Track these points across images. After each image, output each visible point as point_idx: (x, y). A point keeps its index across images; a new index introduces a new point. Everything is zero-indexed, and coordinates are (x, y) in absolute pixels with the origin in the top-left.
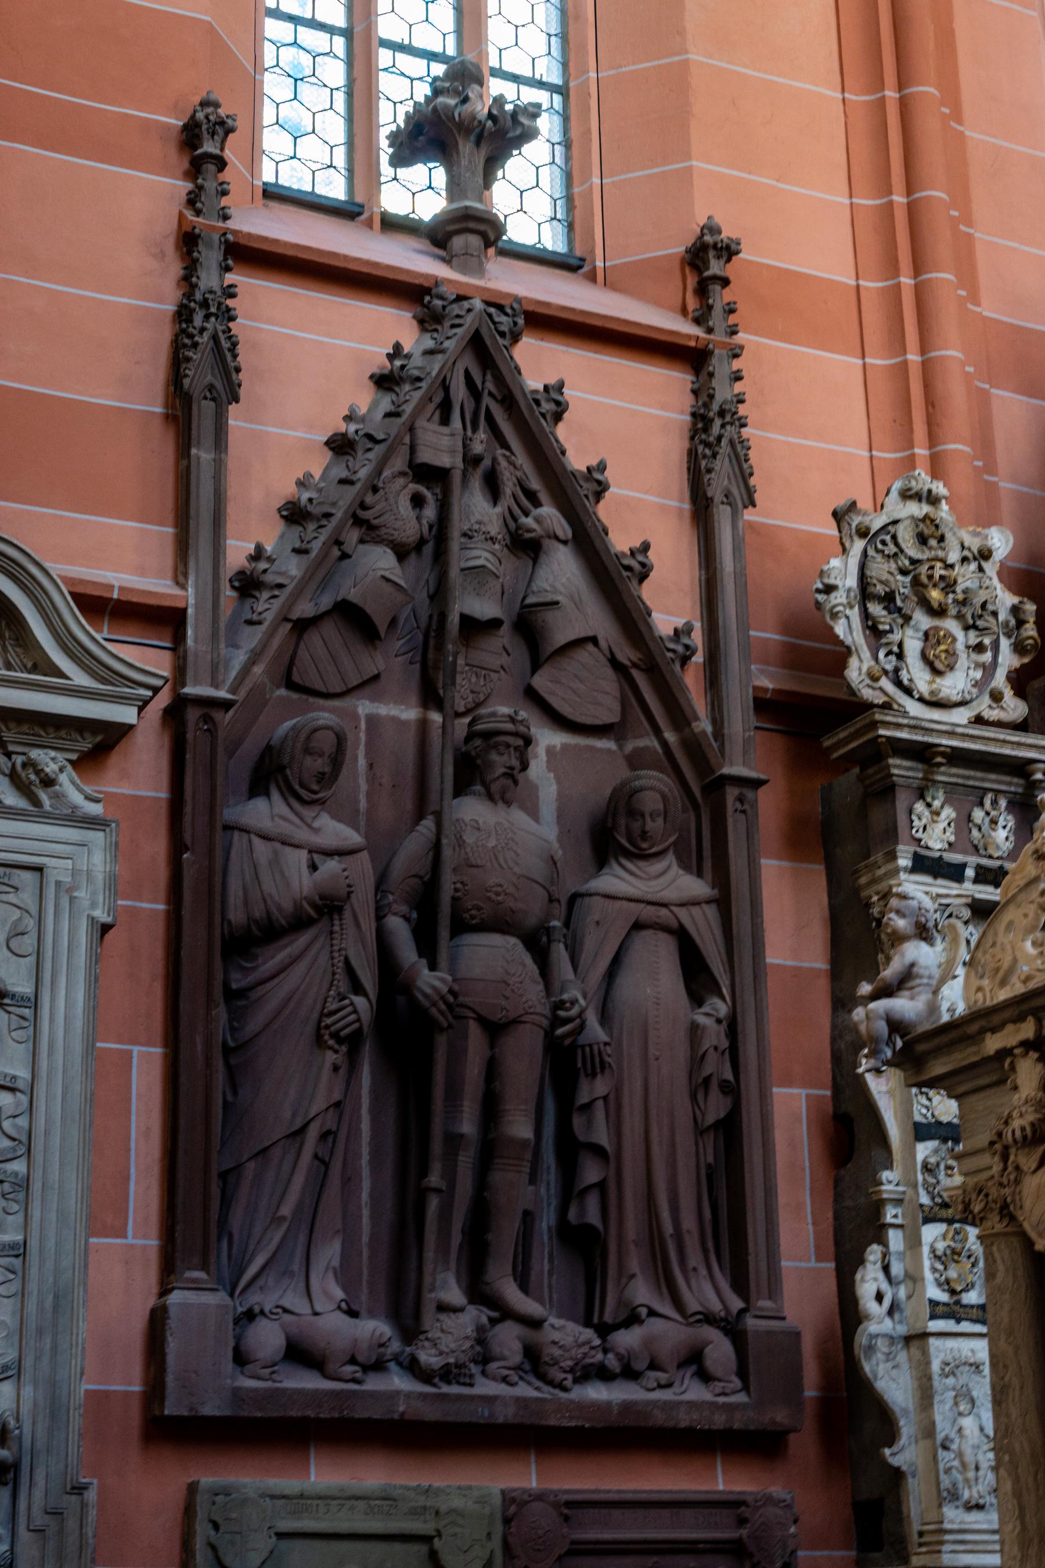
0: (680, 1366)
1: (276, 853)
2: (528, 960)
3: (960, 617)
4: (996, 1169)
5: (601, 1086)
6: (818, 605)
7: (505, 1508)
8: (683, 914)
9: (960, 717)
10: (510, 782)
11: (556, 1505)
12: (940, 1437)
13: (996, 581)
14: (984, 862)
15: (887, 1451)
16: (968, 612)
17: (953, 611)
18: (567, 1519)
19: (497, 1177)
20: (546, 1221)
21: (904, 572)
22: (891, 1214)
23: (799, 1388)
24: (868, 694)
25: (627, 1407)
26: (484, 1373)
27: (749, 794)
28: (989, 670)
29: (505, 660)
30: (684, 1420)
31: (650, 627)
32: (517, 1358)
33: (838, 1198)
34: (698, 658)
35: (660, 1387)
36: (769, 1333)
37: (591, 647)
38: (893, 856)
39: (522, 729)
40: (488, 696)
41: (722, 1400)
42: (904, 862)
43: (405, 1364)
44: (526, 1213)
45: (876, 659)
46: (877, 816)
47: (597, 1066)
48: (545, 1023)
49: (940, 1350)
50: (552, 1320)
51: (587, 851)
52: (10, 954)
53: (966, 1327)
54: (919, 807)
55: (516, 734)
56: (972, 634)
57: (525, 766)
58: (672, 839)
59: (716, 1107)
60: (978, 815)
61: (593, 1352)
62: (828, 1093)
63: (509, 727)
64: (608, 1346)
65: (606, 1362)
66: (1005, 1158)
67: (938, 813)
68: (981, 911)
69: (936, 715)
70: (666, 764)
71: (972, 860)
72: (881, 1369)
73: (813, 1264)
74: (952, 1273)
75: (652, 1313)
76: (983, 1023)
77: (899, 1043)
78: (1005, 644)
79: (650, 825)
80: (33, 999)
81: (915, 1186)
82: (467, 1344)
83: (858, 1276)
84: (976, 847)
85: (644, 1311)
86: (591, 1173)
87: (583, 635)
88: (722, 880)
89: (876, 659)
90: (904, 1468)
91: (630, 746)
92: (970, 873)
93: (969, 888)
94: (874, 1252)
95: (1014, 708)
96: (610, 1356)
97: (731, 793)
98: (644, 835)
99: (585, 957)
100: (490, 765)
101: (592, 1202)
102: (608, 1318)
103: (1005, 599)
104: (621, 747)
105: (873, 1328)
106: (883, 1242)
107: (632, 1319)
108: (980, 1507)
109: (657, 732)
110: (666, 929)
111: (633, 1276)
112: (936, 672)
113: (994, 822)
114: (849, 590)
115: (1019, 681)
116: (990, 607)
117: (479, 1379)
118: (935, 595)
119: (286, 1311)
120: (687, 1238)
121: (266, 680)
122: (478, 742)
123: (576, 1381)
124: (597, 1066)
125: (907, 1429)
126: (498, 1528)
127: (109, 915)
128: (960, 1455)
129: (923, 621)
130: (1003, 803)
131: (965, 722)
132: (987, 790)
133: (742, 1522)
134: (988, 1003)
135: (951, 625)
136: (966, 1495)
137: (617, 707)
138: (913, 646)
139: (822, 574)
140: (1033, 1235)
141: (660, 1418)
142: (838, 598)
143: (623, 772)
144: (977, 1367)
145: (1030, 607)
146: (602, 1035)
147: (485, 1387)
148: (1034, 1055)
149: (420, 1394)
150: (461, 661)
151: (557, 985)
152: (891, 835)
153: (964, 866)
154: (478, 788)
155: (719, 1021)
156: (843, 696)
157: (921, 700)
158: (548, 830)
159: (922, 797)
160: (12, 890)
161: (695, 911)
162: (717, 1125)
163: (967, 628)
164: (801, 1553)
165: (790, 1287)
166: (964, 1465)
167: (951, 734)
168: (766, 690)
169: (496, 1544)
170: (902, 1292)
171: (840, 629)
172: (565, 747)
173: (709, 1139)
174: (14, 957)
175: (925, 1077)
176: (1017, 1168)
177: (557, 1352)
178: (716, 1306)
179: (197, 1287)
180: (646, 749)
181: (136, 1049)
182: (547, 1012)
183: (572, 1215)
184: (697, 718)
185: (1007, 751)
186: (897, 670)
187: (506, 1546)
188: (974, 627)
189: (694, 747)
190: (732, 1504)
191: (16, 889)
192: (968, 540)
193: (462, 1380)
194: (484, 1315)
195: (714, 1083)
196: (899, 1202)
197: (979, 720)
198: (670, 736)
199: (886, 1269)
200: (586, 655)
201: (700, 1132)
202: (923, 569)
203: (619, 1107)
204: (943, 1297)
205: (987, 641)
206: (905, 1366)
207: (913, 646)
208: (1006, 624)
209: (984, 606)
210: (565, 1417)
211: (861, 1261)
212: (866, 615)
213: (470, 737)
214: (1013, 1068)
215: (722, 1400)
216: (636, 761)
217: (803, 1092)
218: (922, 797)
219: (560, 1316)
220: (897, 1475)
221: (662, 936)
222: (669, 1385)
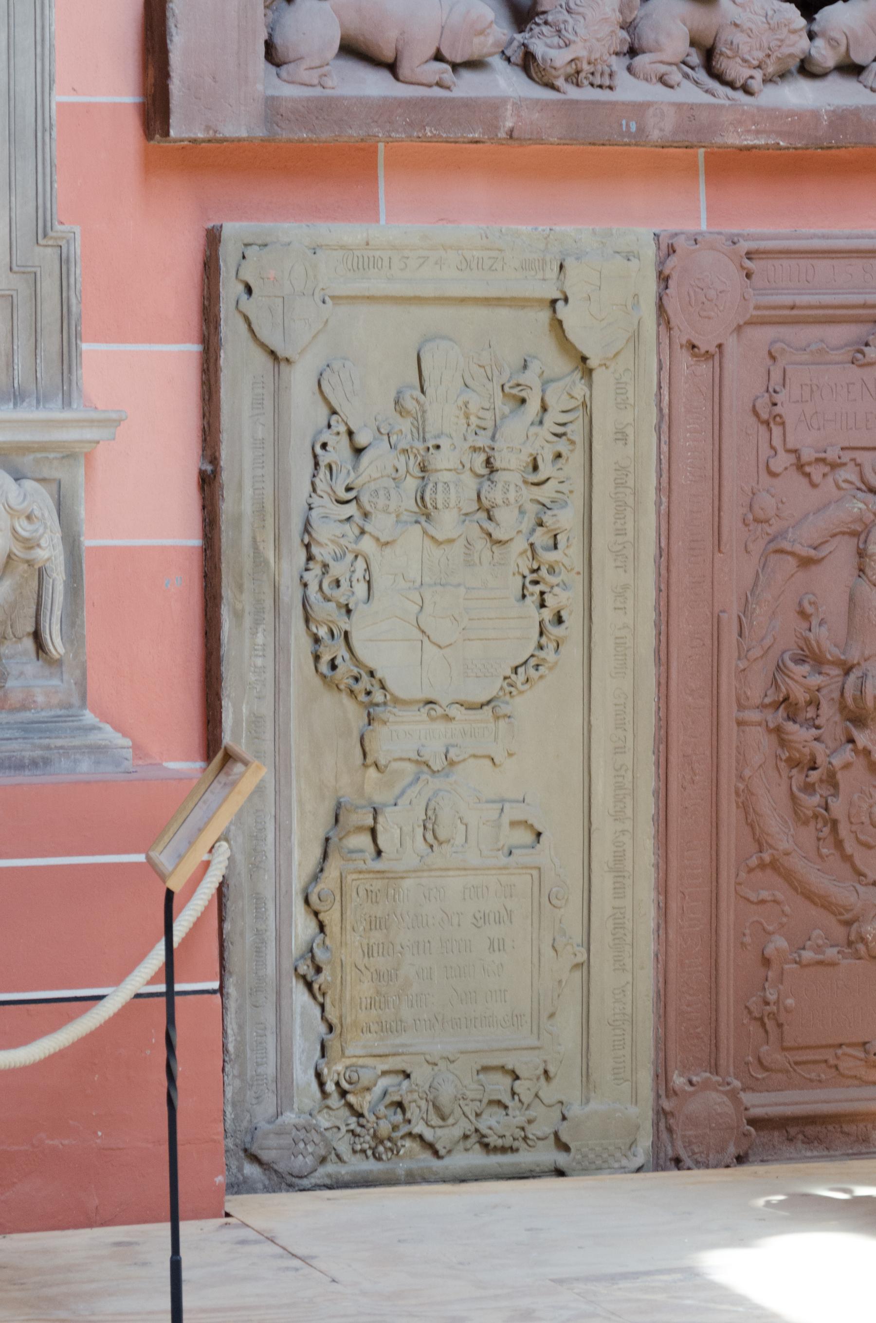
26: (629, 69)
43: (512, 59)
61: (794, 38)
64: (815, 27)
65: (813, 52)
96: (819, 42)
117: (623, 78)
149: (537, 101)
193: (598, 81)
210: (749, 131)
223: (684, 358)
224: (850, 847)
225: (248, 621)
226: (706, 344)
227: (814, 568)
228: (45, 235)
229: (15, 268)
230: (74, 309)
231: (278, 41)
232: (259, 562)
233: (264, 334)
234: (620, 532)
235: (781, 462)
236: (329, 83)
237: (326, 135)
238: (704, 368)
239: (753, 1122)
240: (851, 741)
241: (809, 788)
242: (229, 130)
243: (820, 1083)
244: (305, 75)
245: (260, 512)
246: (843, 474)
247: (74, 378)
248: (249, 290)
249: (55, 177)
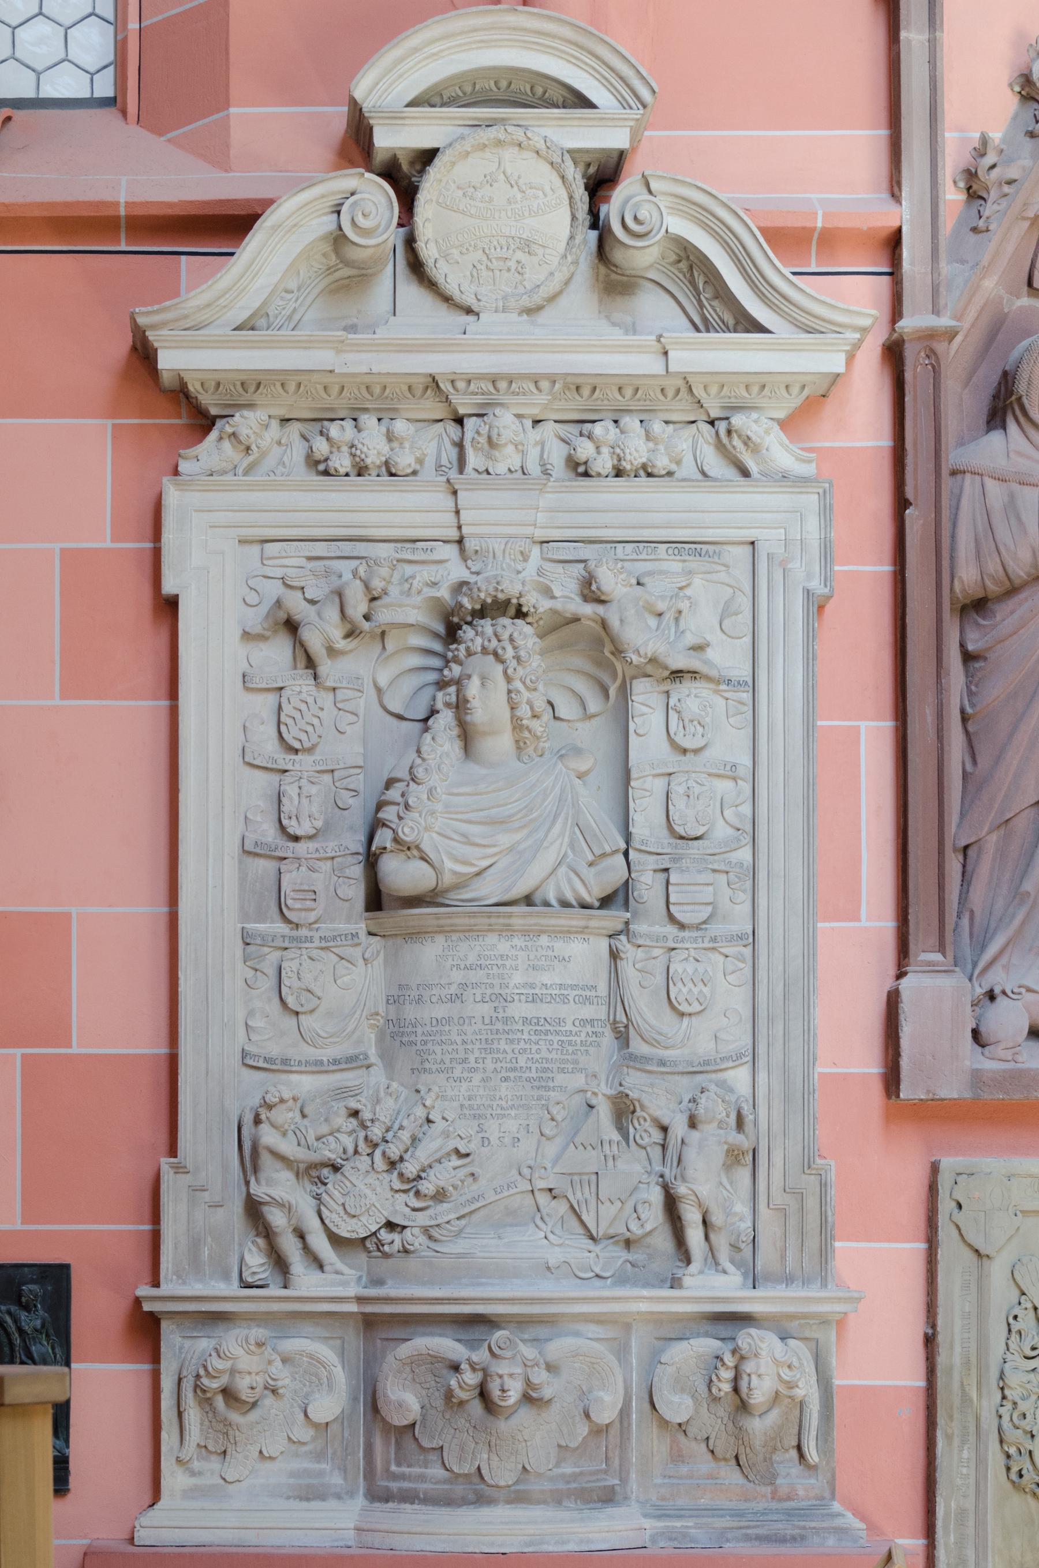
1: (1012, 496)
52: (724, 637)
80: (750, 683)
119: (1029, 990)
121: (1002, 292)
127: (826, 586)
160: (723, 568)
174: (729, 639)
179: (932, 969)
181: (863, 725)
191: (727, 566)
225: (956, 1441)
228: (809, 1168)
229: (787, 1190)
230: (830, 1219)
231: (983, 1029)
232: (965, 1398)
233: (971, 1238)
236: (1020, 1059)
237: (1017, 1096)
242: (945, 1093)
244: (1002, 1054)
245: (967, 1363)
247: (829, 1267)
248: (960, 1206)
249: (817, 1127)
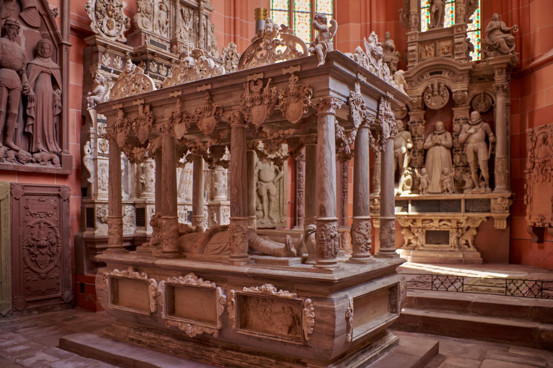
0: (48, 161)
2: (17, 76)
3: (115, 18)
4: (113, 131)
5: (33, 104)
6: (86, 10)
7: (10, 186)
8: (52, 70)
9: (113, 39)
10: (14, 36)
11: (21, 186)
12: (98, 177)
13: (123, 13)
14: (115, 69)
15: (88, 179)
16: (117, 18)
17: (114, 17)
18: (24, 189)
19: (9, 121)
20: (20, 131)
21: (104, 6)
22: (92, 136)
23: (72, 166)
24: (95, 31)
25: (37, 168)
26: (6, 160)
27: (68, 47)
28: (120, 30)
29: (14, 8)
30: (48, 171)
31: (48, 7)
32: (13, 157)
33: (81, 131)
34: (59, 16)
35: (44, 165)
36: (66, 156)
37: (34, 9)
38: (97, 66)
39: (17, 25)
40: (10, 16)
41: (56, 168)
42: (99, 67)
44: (16, 129)
45: (97, 24)
46: (94, 56)
47: (32, 100)
48: (21, 90)
49: (99, 162)
50: (21, 150)
51: (31, 54)
53: (105, 158)
54: (103, 56)
55: (16, 26)
56: (117, 22)
57: (18, 33)
58: (51, 54)
59: (58, 111)
60: (115, 60)
62: (81, 111)
63: (15, 24)
66: (114, 129)
67: (107, 58)
68: (114, 79)
69: (108, 38)
70: (50, 38)
71: (113, 69)
72: (88, 165)
73: (76, 144)
74: (103, 148)
75: (42, 151)
76: (112, 103)
77: (96, 105)
78: (124, 26)
79: (46, 51)
81: (97, 131)
82: (3, 154)
83: (85, 147)
84: (114, 66)
85: (41, 150)
86: (30, 122)
87: (33, 6)
88: (61, 65)
89: (97, 24)
90: (91, 182)
91: (42, 33)
92: (112, 71)
93: (112, 74)
94: (88, 143)
95: (124, 39)
97: (64, 47)
98: (44, 52)
99: (30, 78)
100: (10, 31)
101: (31, 127)
102: (33, 151)
103: (124, 17)
104: (40, 32)
105: (87, 157)
106: (90, 141)
107: (38, 151)
108: (105, 190)
109: (49, 30)
110: (49, 74)
111: (39, 143)
112: (109, 29)
113: (118, 62)
114: (92, 8)
115: (126, 34)
116: (121, 17)
117: (5, 161)
118: (110, 13)
120: (50, 137)
122: (7, 26)
123: (26, 163)
124: (32, 100)
125: (92, 175)
126: (9, 190)
128: (102, 181)
129: (107, 17)
130: (120, 58)
131: (114, 40)
132: (117, 55)
133: (60, 190)
134: (114, 100)
135: (113, 20)
136: (103, 188)
137: (40, 23)
138: (105, 23)
139: (87, 3)
140: (119, 144)
141: (43, 171)
142: (90, 9)
143: (40, 38)
144: (106, 165)
145: (129, 19)
146: (34, 94)
147: (6, 163)
148: (122, 111)
150: (3, 7)
151: (24, 82)
152: (97, 61)
153: (111, 70)
154: (7, 36)
155: (59, 94)
156: (90, 30)
157: (106, 34)
158: (23, 48)
159: (104, 54)
161: (55, 71)
162: (58, 115)
163: (116, 21)
164: (71, 197)
165: (71, 147)
166: (103, 183)
167: (111, 43)
168: (73, 26)
169: (9, 193)
170: (93, 151)
171: (90, 16)
172: (27, 30)
173: (56, 118)
175: (100, 112)
176: (117, 131)
177: (22, 157)
178: (56, 150)
180: (46, 34)
182: (22, 88)
183: (26, 130)
184: (58, 29)
185: (122, 48)
186: (101, 27)
187: (11, 193)
188: (118, 21)
189: (56, 35)
190: (58, 188)
192: (118, 2)
194: (6, 148)
195: (57, 107)
196: (93, 134)
197: (117, 41)
198: (51, 32)
199: (90, 146)
200: (33, 10)
201: (54, 116)
202: (108, 7)
203: (37, 109)
204: (101, 152)
205: (120, 24)
206: (93, 164)
207: (105, 23)
208: (124, 22)
209: (120, 17)
211: (85, 144)
212: (96, 14)
213: (5, 24)
214: (117, 112)
215: (56, 168)
216: (43, 36)
217: (76, 110)
218: (104, 54)
219: (23, 150)
220: (90, 184)
221: (47, 75)
222: (46, 165)
223: (14, 200)
224: (39, 265)
226: (17, 198)
227: (33, 228)
234: (5, 223)
235: (28, 214)
238: (17, 201)
239: (27, 302)
240: (39, 250)
241: (33, 257)
243: (36, 296)
246: (37, 216)
